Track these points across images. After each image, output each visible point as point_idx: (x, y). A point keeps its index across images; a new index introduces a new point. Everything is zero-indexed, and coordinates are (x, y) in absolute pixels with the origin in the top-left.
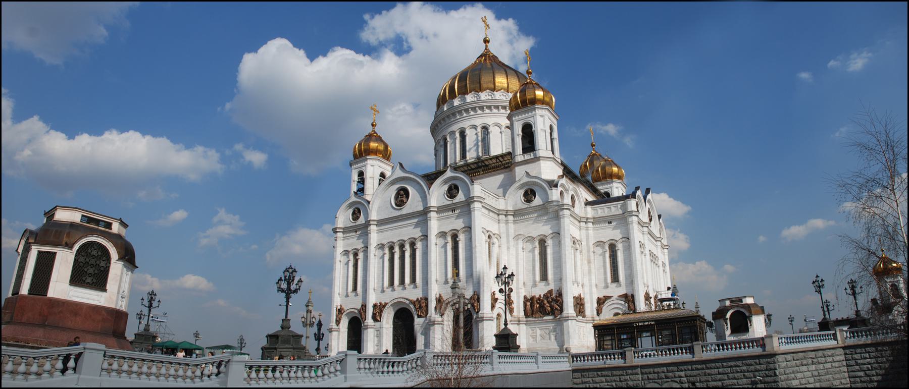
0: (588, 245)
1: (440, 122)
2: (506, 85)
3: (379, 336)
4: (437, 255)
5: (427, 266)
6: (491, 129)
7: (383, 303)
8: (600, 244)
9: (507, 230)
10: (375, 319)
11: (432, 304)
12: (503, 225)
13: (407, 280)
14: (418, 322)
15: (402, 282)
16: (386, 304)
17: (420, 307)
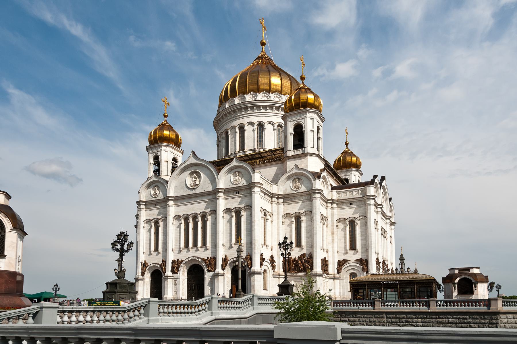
0: (332, 221)
1: (222, 117)
2: (280, 88)
3: (176, 284)
4: (224, 226)
5: (216, 234)
6: (266, 126)
7: (180, 260)
8: (341, 220)
9: (278, 209)
10: (173, 271)
11: (220, 262)
12: (275, 205)
13: (200, 243)
14: (208, 275)
15: (195, 245)
16: (182, 261)
17: (210, 264)
